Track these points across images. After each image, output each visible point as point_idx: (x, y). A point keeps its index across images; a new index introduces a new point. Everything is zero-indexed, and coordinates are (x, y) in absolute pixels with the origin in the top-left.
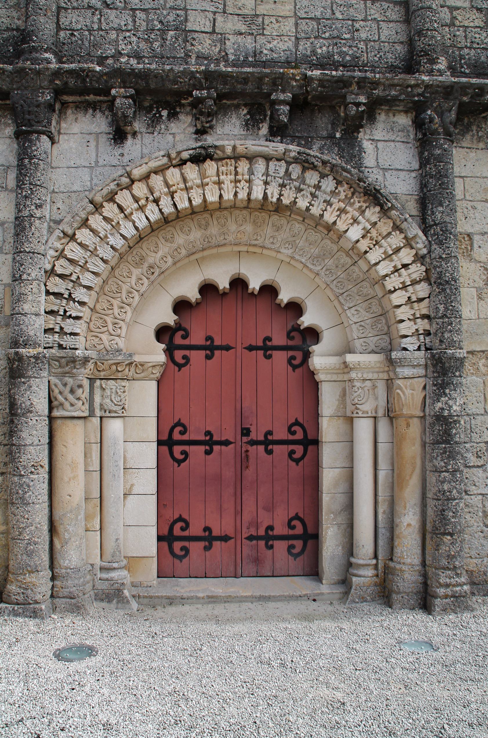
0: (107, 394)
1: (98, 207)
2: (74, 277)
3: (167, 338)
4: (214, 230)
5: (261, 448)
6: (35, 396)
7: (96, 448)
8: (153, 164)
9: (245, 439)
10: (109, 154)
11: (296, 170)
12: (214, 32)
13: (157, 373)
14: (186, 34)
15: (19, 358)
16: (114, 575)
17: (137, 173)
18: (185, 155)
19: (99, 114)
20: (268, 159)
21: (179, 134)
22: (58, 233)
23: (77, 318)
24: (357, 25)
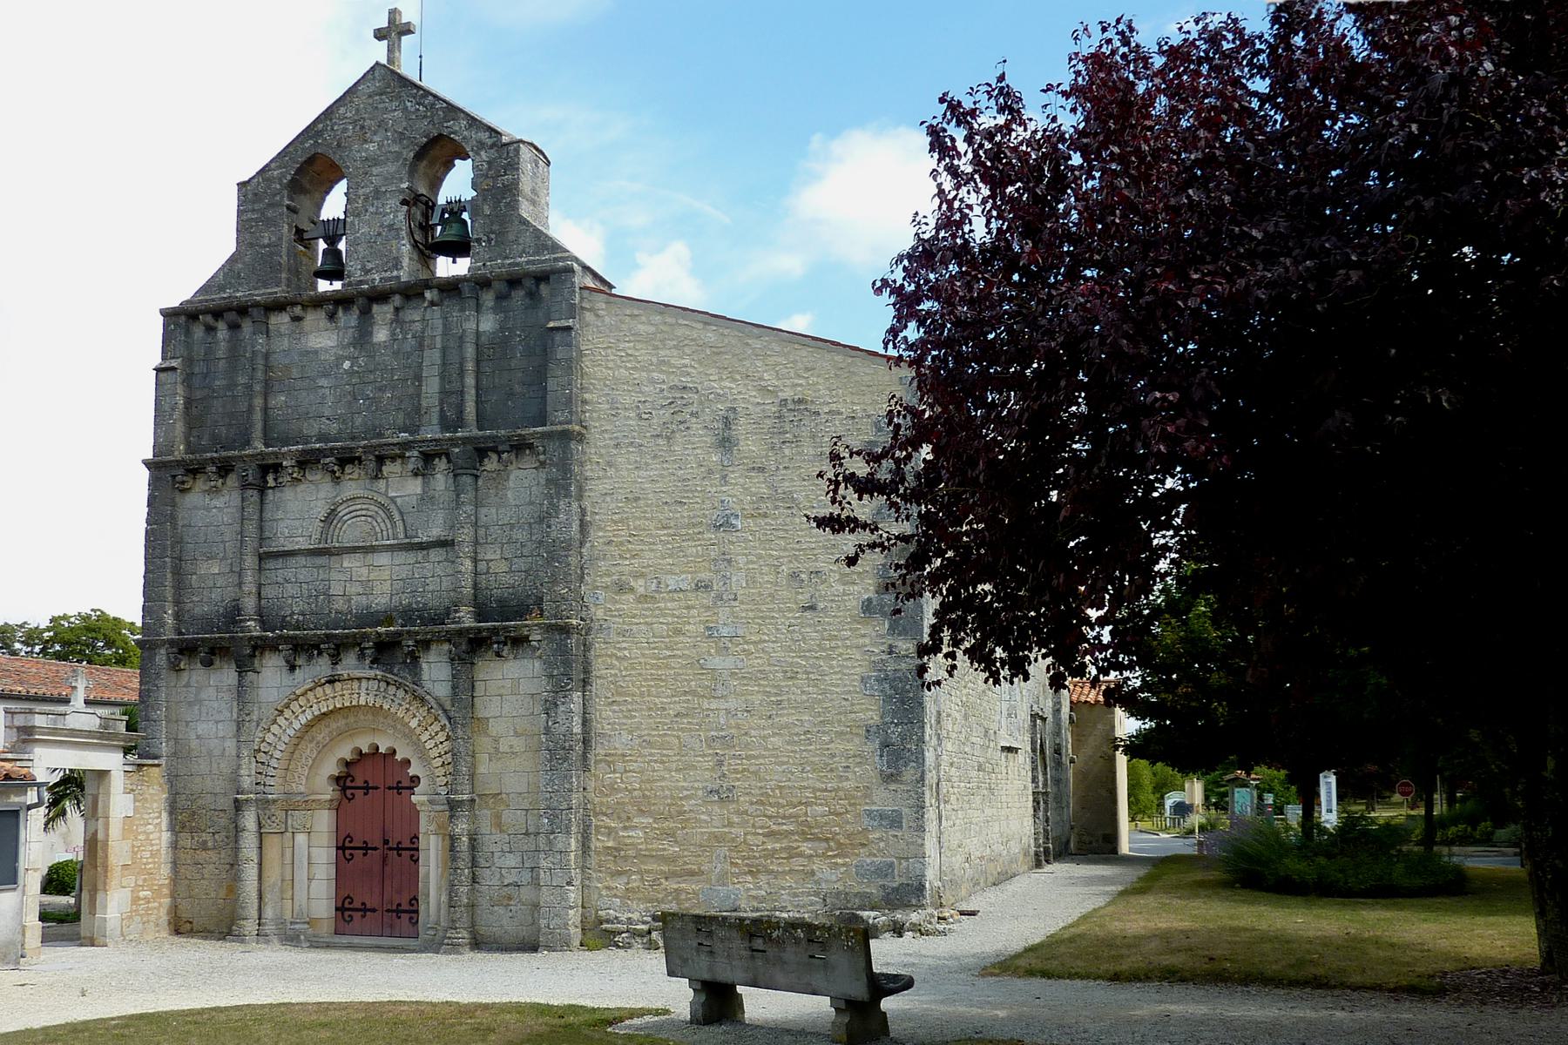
0: (297, 818)
4: (351, 719)
6: (249, 821)
11: (383, 685)
15: (236, 800)
21: (322, 667)
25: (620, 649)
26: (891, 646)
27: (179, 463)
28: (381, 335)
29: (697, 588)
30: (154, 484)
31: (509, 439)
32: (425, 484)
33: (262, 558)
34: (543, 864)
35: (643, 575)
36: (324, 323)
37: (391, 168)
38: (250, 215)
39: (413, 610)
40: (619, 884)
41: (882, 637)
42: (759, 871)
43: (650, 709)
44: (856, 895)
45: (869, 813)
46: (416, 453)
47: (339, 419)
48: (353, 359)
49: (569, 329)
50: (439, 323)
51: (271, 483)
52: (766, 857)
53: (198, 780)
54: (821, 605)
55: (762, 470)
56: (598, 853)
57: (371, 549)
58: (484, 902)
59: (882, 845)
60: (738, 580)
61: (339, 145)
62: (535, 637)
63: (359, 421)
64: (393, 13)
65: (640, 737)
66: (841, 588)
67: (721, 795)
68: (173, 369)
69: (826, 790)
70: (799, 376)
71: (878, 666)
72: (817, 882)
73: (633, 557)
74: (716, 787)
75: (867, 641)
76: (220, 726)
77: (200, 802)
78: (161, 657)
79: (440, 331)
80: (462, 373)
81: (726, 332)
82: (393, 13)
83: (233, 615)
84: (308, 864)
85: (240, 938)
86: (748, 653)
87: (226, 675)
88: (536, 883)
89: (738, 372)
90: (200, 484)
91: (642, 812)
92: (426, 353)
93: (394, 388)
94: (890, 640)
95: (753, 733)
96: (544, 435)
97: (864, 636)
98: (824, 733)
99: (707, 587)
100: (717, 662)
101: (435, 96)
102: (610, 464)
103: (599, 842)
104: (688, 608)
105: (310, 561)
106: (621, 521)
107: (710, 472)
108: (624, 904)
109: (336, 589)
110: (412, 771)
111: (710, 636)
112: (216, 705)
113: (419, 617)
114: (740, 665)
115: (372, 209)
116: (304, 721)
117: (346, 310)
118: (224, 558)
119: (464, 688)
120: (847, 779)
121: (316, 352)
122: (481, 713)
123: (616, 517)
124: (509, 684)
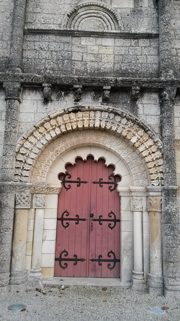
0: (38, 200)
2: (27, 155)
3: (62, 178)
5: (98, 222)
7: (32, 221)
8: (58, 113)
9: (91, 218)
10: (41, 108)
12: (82, 61)
13: (58, 191)
16: (36, 275)
18: (70, 110)
19: (38, 93)
20: (101, 111)
21: (68, 102)
22: (21, 138)
23: (28, 170)
24: (138, 57)
105: (58, 38)
109: (76, 57)
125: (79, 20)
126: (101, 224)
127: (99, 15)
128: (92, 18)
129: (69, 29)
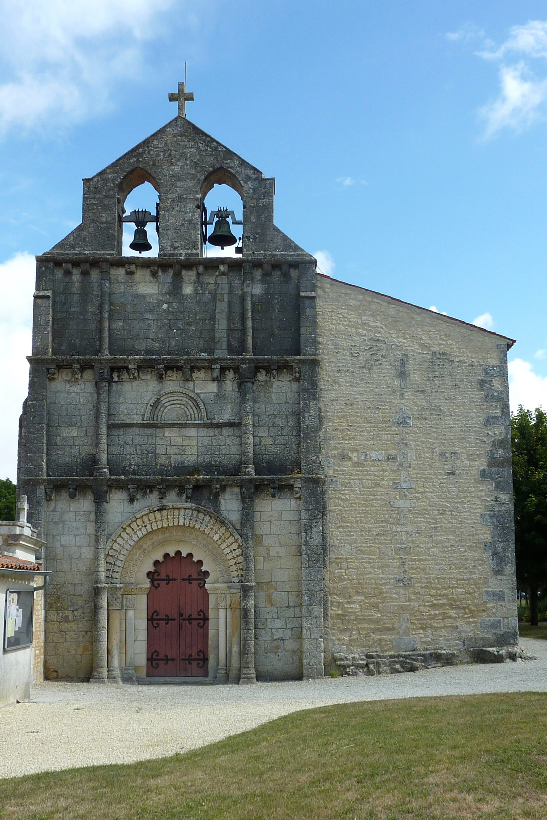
1: (124, 529)
2: (116, 557)
4: (167, 534)
5: (187, 622)
7: (124, 621)
8: (144, 513)
9: (181, 618)
10: (128, 508)
12: (166, 454)
13: (147, 591)
14: (156, 455)
16: (130, 671)
17: (138, 516)
18: (155, 509)
21: (153, 499)
22: (110, 540)
23: (117, 572)
25: (343, 494)
26: (496, 497)
27: (52, 361)
28: (188, 290)
29: (388, 459)
30: (33, 373)
31: (278, 362)
32: (219, 387)
33: (110, 427)
34: (305, 625)
35: (356, 450)
36: (148, 278)
37: (190, 184)
38: (92, 201)
39: (213, 466)
40: (345, 637)
41: (491, 491)
42: (427, 627)
43: (362, 531)
44: (481, 639)
45: (487, 592)
46: (219, 367)
47: (160, 340)
48: (170, 304)
49: (314, 298)
50: (226, 286)
51: (116, 379)
52: (430, 619)
53: (62, 575)
54: (457, 472)
55: (423, 392)
56: (332, 618)
57: (186, 426)
58: (261, 651)
59: (494, 610)
60: (411, 455)
61: (154, 164)
62: (298, 485)
63: (173, 343)
64: (181, 86)
65: (356, 547)
66: (468, 463)
67: (404, 583)
68: (48, 297)
69: (463, 580)
70: (441, 339)
71: (491, 508)
72: (460, 633)
73: (350, 439)
74: (401, 578)
75: (483, 494)
76: (78, 538)
77: (63, 590)
78: (41, 491)
79: (226, 291)
80: (243, 318)
81: (401, 309)
82: (181, 86)
83: (92, 463)
84: (130, 631)
85: (100, 680)
86: (418, 499)
87: (85, 504)
88: (299, 637)
89: (408, 334)
90: (65, 375)
91: (358, 593)
92: (218, 304)
93: (197, 324)
94: (495, 494)
95: (422, 545)
96: (300, 361)
97: (481, 491)
98: (462, 546)
99: (394, 459)
100: (401, 503)
101: (218, 143)
102: (335, 382)
103: (334, 611)
104: (383, 471)
105: (142, 431)
106: (343, 417)
107: (394, 391)
108: (348, 649)
109: (160, 450)
110: (204, 569)
111: (396, 488)
112: (74, 524)
113: (216, 470)
114: (413, 505)
115: (177, 208)
116: (140, 535)
117: (164, 271)
118: (81, 426)
119: (247, 516)
120: (475, 573)
121: (144, 296)
122: (259, 532)
123: (339, 414)
124: (277, 514)
125: (162, 409)
126: (190, 623)
127: (182, 403)
128: (175, 406)
129: (152, 422)
